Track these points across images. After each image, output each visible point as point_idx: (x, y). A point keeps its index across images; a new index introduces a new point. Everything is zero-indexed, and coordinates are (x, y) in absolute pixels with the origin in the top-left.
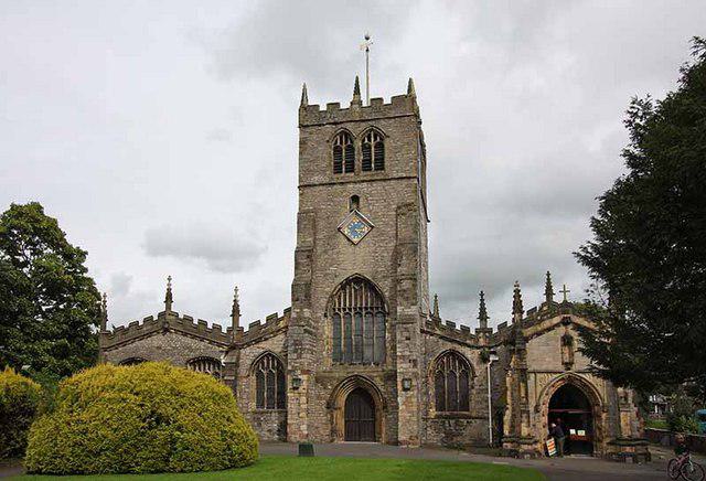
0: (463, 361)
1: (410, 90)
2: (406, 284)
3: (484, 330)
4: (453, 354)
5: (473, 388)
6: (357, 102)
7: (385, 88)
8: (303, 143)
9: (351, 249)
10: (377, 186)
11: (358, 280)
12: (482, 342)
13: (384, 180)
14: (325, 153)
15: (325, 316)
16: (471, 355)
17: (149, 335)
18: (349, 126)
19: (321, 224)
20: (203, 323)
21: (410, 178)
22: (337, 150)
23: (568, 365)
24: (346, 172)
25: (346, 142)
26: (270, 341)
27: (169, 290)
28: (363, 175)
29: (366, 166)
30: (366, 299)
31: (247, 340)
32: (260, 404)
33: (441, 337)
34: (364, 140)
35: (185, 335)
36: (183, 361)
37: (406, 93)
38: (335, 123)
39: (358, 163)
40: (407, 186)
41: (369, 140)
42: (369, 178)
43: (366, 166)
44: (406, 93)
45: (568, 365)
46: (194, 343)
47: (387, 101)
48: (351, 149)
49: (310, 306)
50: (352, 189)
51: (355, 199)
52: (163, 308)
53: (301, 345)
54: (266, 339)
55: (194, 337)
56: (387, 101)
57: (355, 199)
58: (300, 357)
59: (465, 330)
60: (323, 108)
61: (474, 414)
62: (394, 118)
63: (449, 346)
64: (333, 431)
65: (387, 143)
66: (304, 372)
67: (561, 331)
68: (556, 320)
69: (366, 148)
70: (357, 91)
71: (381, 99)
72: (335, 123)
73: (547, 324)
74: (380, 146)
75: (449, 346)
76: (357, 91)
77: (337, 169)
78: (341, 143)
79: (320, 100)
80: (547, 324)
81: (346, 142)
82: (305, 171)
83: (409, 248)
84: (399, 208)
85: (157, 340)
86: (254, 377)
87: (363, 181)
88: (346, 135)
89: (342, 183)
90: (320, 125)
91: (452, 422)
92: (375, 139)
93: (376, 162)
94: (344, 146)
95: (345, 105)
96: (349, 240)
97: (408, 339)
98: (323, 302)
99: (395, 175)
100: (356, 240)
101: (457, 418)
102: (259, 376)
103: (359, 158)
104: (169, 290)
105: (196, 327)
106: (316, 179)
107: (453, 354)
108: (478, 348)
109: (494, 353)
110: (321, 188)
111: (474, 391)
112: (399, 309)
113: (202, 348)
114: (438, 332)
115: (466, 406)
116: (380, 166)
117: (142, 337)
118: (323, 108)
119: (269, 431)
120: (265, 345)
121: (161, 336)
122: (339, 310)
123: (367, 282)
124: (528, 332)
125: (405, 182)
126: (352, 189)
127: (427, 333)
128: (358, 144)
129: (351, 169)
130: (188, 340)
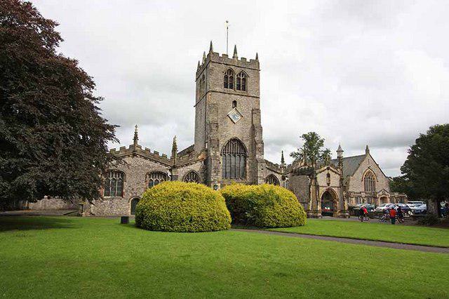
1: (257, 58)
4: (272, 175)
7: (246, 53)
11: (235, 140)
18: (233, 67)
20: (156, 153)
22: (226, 77)
23: (328, 184)
26: (192, 166)
27: (136, 133)
30: (238, 149)
31: (181, 164)
35: (146, 158)
38: (227, 65)
43: (239, 86)
45: (328, 184)
46: (152, 164)
47: (248, 60)
48: (232, 78)
50: (234, 97)
55: (151, 160)
56: (248, 60)
57: (235, 102)
58: (217, 175)
63: (271, 173)
66: (219, 182)
67: (327, 171)
68: (326, 168)
69: (239, 79)
72: (227, 65)
73: (323, 169)
74: (244, 80)
75: (271, 173)
80: (323, 169)
83: (256, 129)
88: (230, 71)
93: (243, 87)
104: (136, 133)
105: (153, 155)
106: (218, 89)
107: (272, 176)
112: (257, 156)
113: (156, 167)
116: (244, 89)
118: (221, 55)
120: (191, 167)
121: (130, 158)
123: (239, 141)
124: (317, 171)
126: (234, 97)
129: (231, 87)
130: (148, 162)
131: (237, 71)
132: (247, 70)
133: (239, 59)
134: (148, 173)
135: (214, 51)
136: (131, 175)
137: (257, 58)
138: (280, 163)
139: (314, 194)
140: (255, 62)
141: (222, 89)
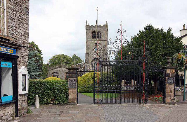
1: (106, 24)
7: (102, 23)
14: (91, 35)
17: (58, 68)
18: (95, 30)
19: (90, 48)
29: (98, 38)
35: (65, 68)
39: (97, 37)
56: (102, 25)
74: (101, 34)
77: (93, 38)
82: (87, 38)
88: (94, 31)
106: (89, 40)
116: (101, 38)
117: (56, 68)
126: (96, 42)
128: (97, 34)
129: (95, 38)
131: (97, 31)
133: (98, 25)
140: (106, 26)
141: (91, 39)
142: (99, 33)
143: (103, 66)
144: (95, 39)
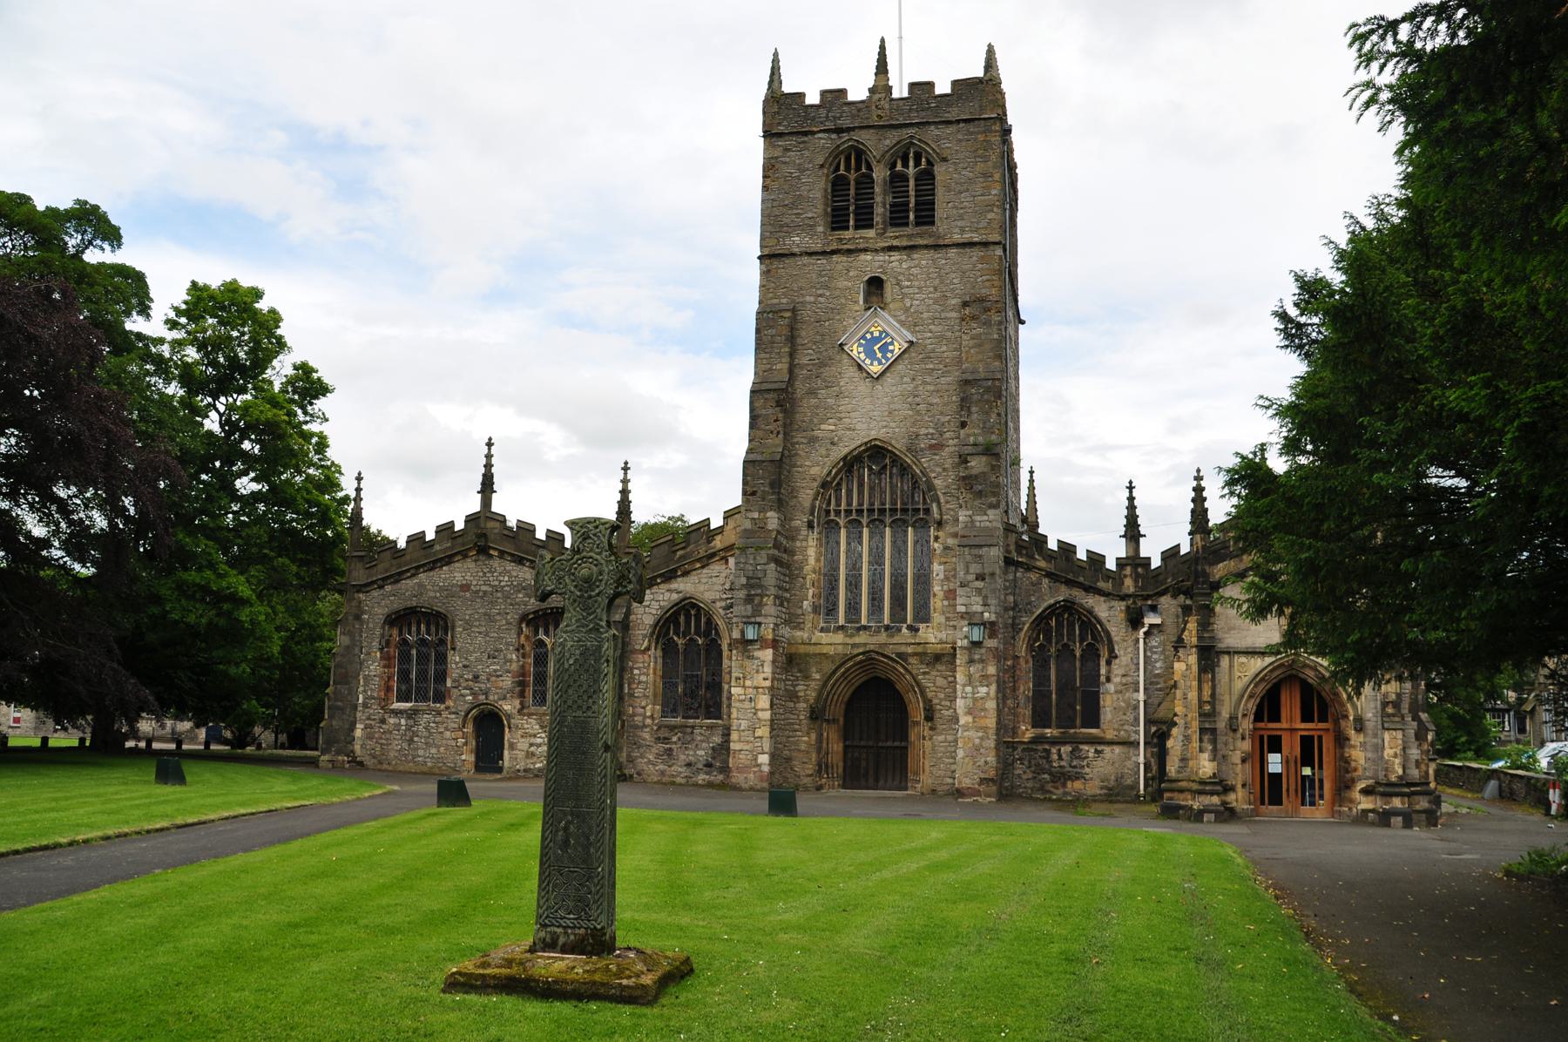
0: (1090, 625)
1: (990, 63)
2: (977, 464)
3: (1135, 561)
4: (1069, 607)
5: (1108, 680)
6: (881, 87)
8: (769, 169)
9: (863, 387)
10: (923, 259)
11: (876, 453)
12: (1129, 585)
13: (936, 247)
14: (816, 188)
15: (810, 526)
16: (1109, 613)
17: (448, 560)
18: (866, 138)
21: (985, 244)
22: (838, 184)
24: (857, 227)
25: (858, 168)
26: (693, 578)
28: (894, 236)
29: (897, 217)
30: (891, 490)
32: (669, 707)
33: (1049, 575)
34: (894, 165)
36: (513, 617)
37: (981, 74)
38: (839, 131)
39: (880, 212)
40: (982, 260)
41: (906, 165)
42: (905, 243)
44: (981, 74)
47: (943, 88)
48: (866, 182)
49: (780, 505)
50: (870, 264)
51: (875, 286)
52: (474, 505)
53: (761, 586)
54: (686, 574)
56: (943, 88)
57: (875, 286)
59: (1096, 560)
60: (813, 98)
61: (1110, 735)
62: (958, 122)
63: (1063, 593)
64: (822, 767)
65: (940, 171)
69: (897, 180)
70: (882, 67)
71: (930, 85)
72: (839, 131)
74: (926, 177)
75: (1063, 593)
76: (882, 67)
77: (838, 221)
78: (848, 169)
79: (807, 82)
81: (858, 168)
82: (774, 223)
84: (965, 304)
85: (461, 572)
86: (659, 653)
87: (891, 248)
88: (858, 155)
89: (849, 252)
90: (805, 134)
91: (1066, 749)
92: (917, 163)
94: (852, 176)
95: (858, 92)
96: (860, 367)
97: (981, 577)
98: (806, 495)
99: (957, 238)
100: (876, 369)
101: (1076, 742)
102: (669, 650)
103: (881, 204)
106: (797, 241)
107: (1069, 607)
108: (1123, 598)
109: (1154, 609)
110: (806, 260)
111: (1111, 687)
114: (1042, 564)
115: (1093, 718)
116: (926, 215)
118: (813, 98)
119: (689, 765)
120: (685, 586)
121: (470, 564)
122: (838, 513)
125: (976, 253)
127: (1018, 564)
128: (880, 174)
129: (865, 222)
131: (877, 145)
132: (934, 131)
133: (900, 91)
134: (524, 618)
135: (788, 87)
136: (468, 625)
137: (990, 63)
138: (1114, 551)
139: (1193, 696)
142: (911, 171)
143: (1225, 661)
144: (871, 233)
